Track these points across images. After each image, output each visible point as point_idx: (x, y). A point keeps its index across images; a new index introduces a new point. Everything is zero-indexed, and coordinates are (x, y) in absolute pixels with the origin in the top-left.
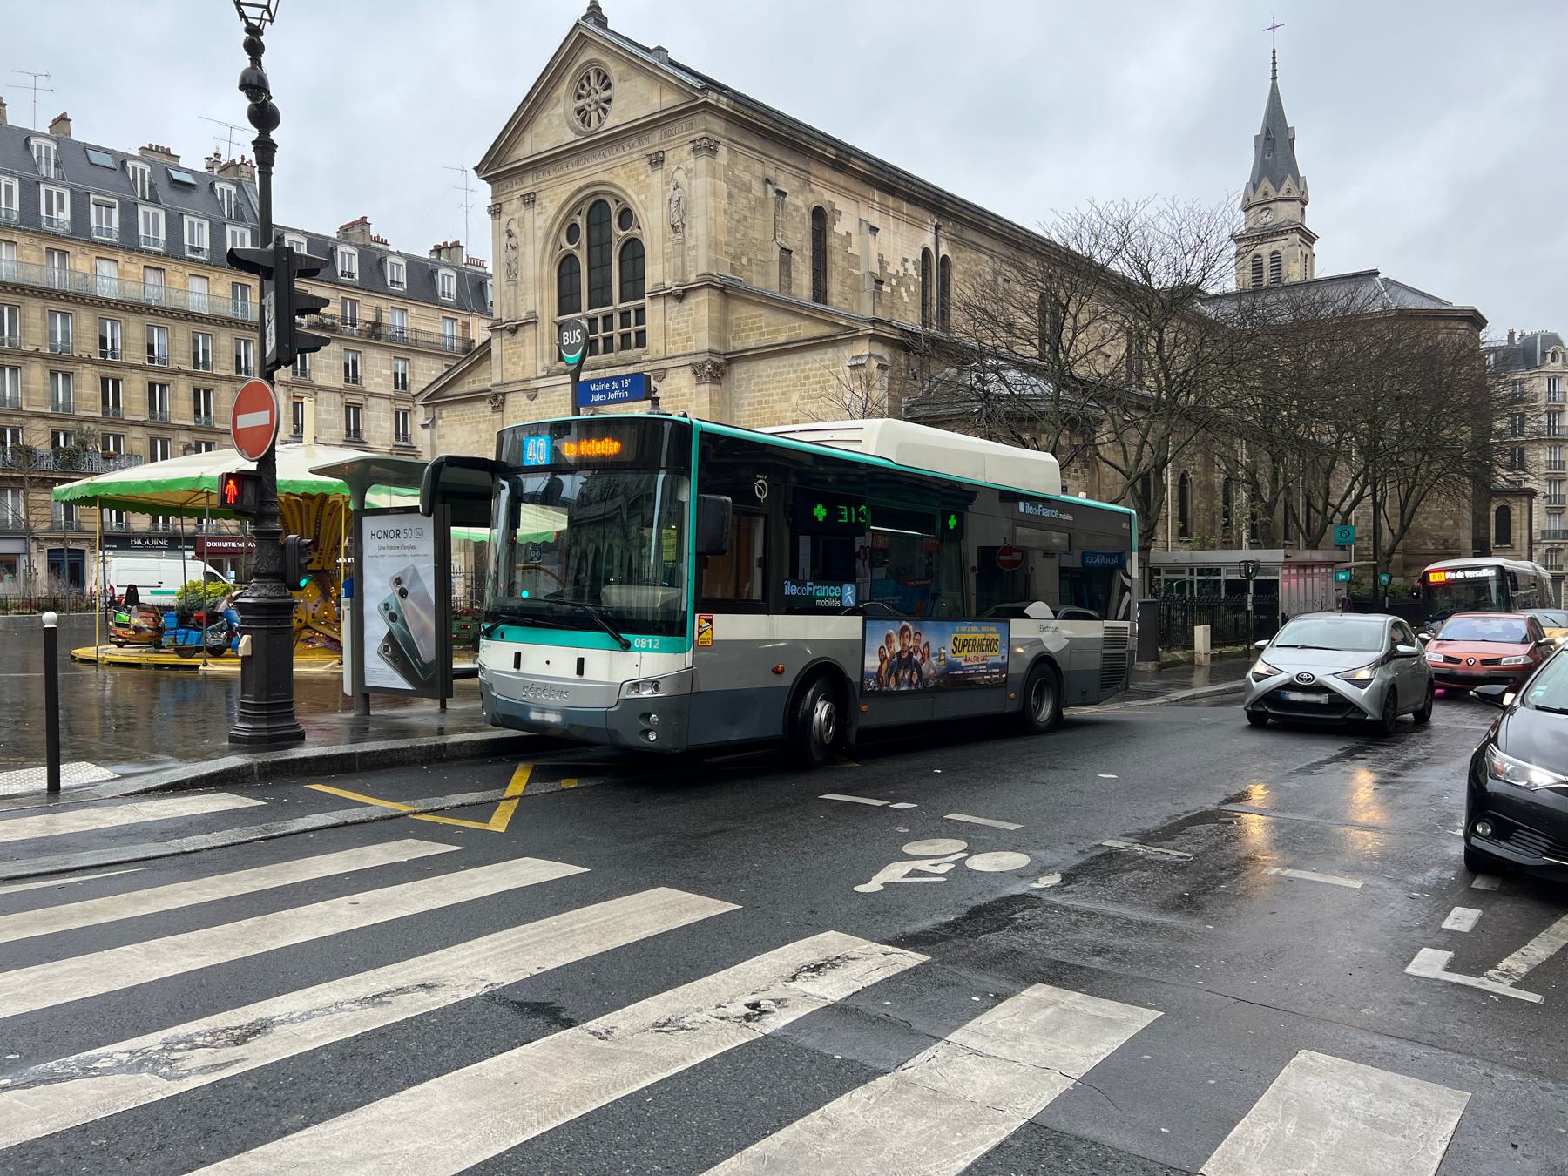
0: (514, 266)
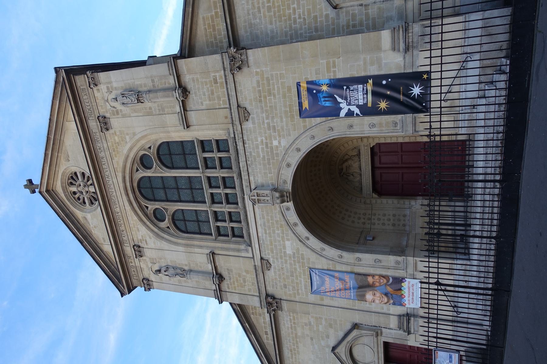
0: (179, 271)
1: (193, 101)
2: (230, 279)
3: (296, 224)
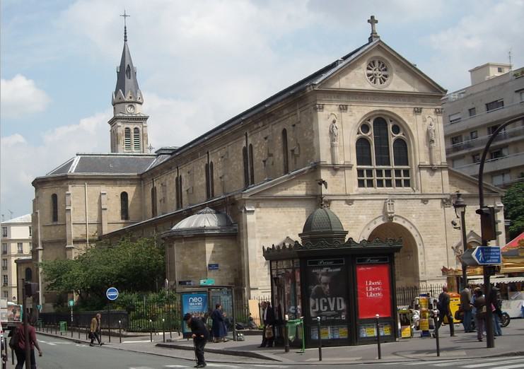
3: (375, 223)
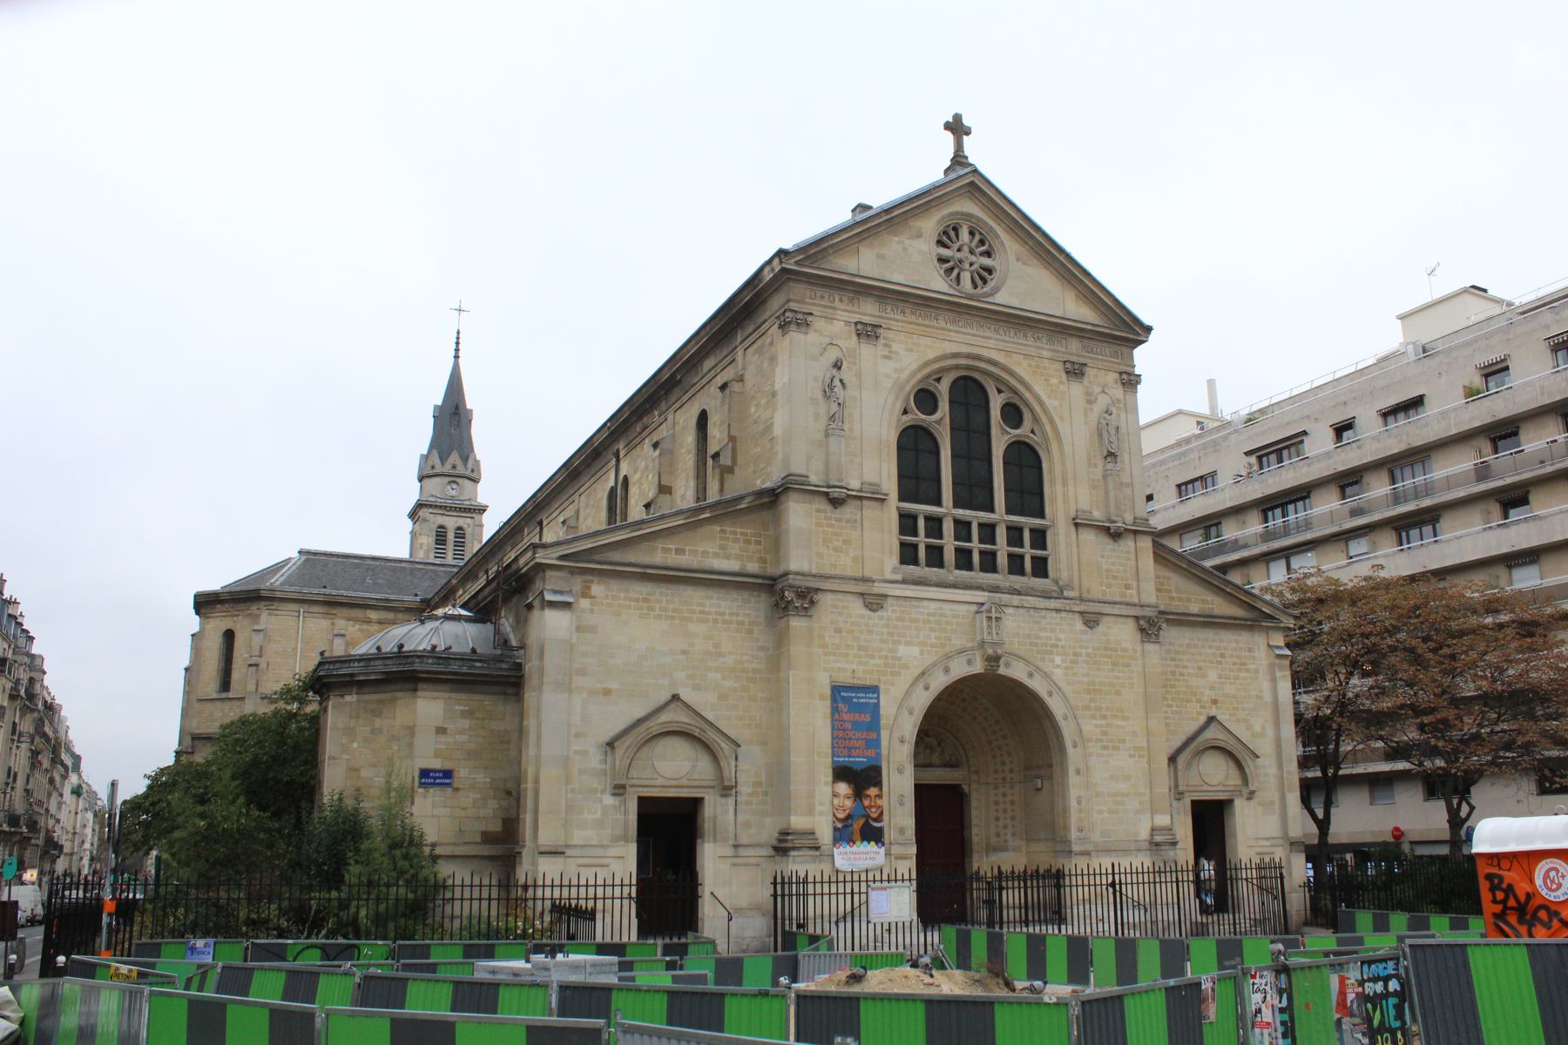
1: (1105, 540)
2: (839, 520)
3: (947, 670)
